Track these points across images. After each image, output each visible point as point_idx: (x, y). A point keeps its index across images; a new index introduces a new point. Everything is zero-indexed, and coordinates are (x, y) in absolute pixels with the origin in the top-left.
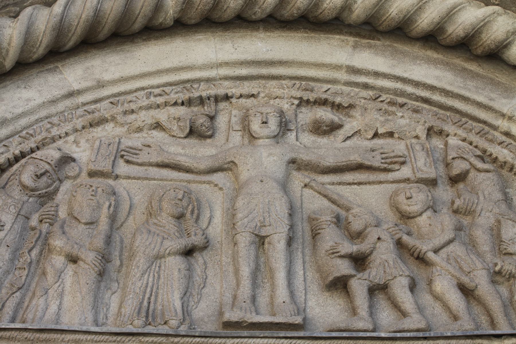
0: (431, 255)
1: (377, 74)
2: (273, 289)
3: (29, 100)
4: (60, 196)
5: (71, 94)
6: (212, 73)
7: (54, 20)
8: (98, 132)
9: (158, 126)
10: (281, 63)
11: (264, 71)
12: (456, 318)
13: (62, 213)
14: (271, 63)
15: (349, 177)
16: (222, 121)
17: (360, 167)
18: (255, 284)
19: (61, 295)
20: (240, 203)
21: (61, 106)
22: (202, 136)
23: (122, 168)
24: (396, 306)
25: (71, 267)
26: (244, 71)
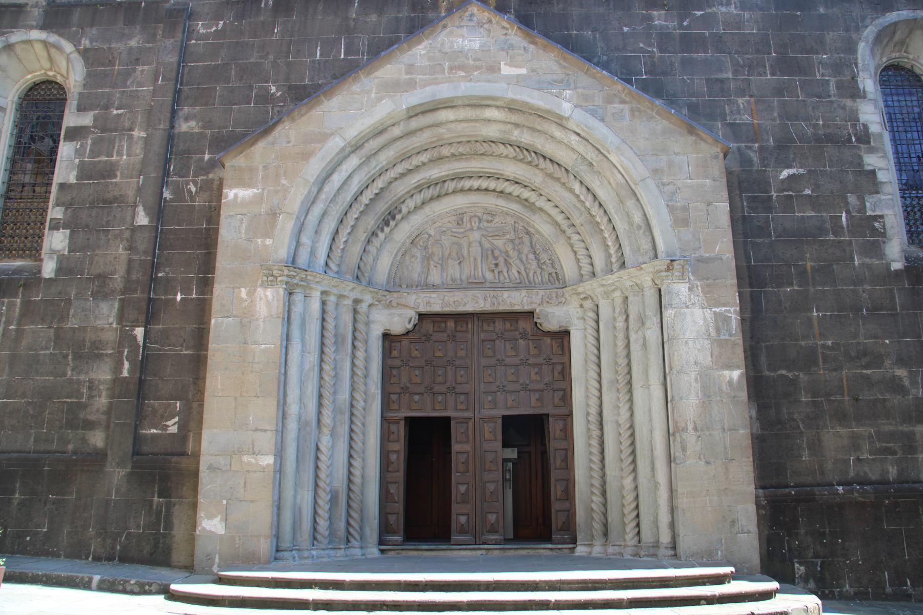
0: (512, 263)
1: (502, 207)
2: (478, 272)
3: (418, 219)
4: (429, 246)
5: (427, 216)
6: (461, 206)
7: (422, 200)
8: (435, 225)
9: (449, 222)
10: (479, 203)
11: (474, 205)
12: (516, 279)
13: (430, 252)
14: (476, 203)
15: (495, 238)
16: (465, 219)
17: (497, 235)
18: (475, 270)
19: (434, 275)
20: (470, 249)
21: (425, 220)
22: (460, 225)
23: (443, 237)
24: (504, 276)
25: (435, 268)
26: (469, 205)
